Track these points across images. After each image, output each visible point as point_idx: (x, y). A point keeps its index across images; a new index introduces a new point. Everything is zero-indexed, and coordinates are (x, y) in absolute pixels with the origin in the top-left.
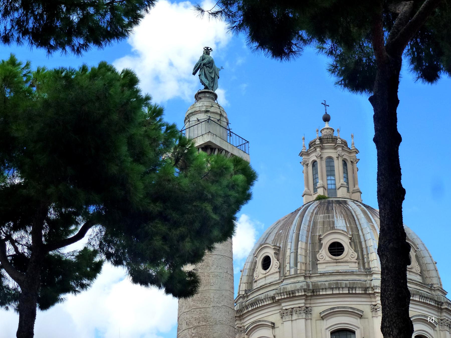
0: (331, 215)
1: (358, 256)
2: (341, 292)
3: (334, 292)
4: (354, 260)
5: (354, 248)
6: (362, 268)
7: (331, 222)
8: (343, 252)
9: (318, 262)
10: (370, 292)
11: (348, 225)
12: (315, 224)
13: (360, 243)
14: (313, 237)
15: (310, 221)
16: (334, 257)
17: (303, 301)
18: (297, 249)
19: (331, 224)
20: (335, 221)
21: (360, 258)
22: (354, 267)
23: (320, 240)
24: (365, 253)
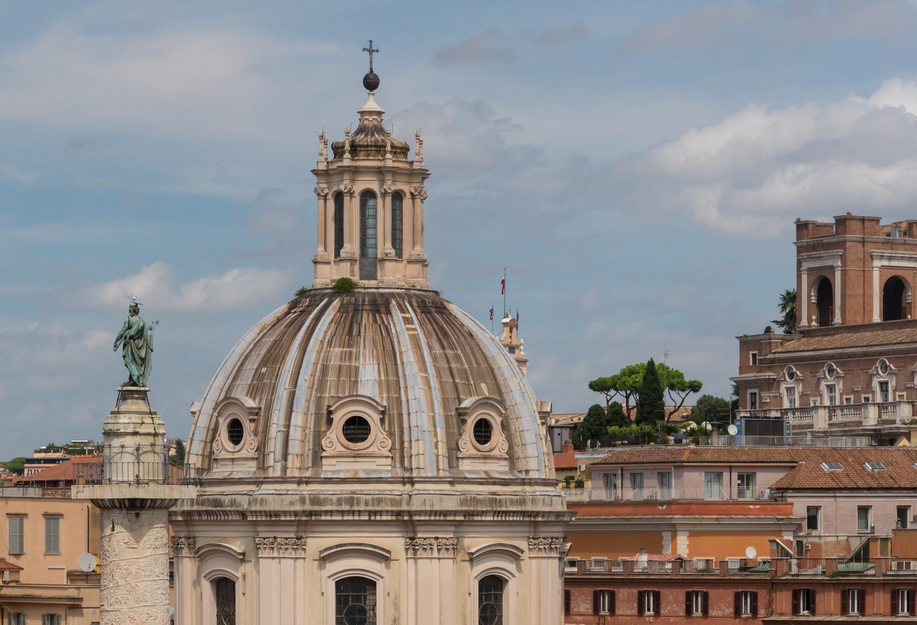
0: (354, 350)
1: (393, 444)
2: (356, 518)
3: (346, 518)
4: (385, 452)
5: (387, 429)
6: (398, 465)
7: (353, 370)
8: (364, 439)
9: (324, 454)
10: (406, 518)
11: (383, 378)
12: (325, 370)
13: (400, 415)
14: (319, 400)
15: (316, 364)
16: (352, 445)
17: (294, 529)
18: (288, 426)
19: (353, 374)
20: (361, 366)
21: (398, 446)
22: (383, 467)
23: (330, 413)
24: (406, 438)
